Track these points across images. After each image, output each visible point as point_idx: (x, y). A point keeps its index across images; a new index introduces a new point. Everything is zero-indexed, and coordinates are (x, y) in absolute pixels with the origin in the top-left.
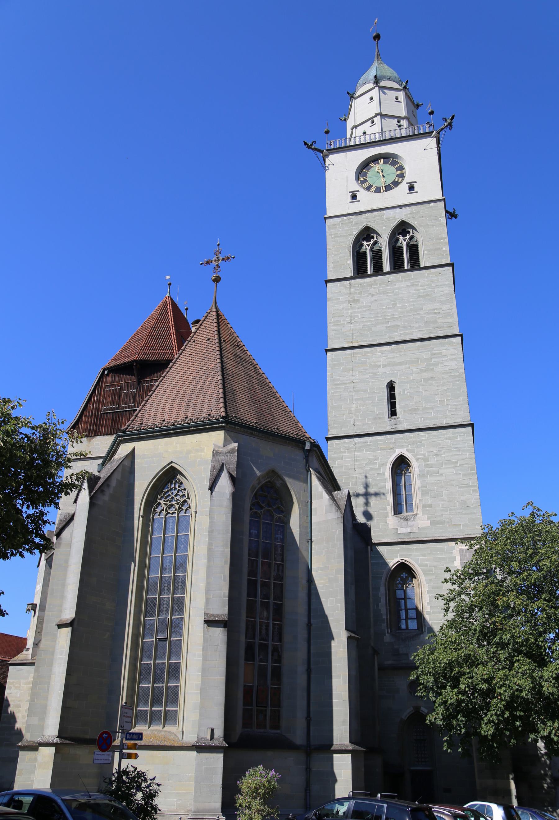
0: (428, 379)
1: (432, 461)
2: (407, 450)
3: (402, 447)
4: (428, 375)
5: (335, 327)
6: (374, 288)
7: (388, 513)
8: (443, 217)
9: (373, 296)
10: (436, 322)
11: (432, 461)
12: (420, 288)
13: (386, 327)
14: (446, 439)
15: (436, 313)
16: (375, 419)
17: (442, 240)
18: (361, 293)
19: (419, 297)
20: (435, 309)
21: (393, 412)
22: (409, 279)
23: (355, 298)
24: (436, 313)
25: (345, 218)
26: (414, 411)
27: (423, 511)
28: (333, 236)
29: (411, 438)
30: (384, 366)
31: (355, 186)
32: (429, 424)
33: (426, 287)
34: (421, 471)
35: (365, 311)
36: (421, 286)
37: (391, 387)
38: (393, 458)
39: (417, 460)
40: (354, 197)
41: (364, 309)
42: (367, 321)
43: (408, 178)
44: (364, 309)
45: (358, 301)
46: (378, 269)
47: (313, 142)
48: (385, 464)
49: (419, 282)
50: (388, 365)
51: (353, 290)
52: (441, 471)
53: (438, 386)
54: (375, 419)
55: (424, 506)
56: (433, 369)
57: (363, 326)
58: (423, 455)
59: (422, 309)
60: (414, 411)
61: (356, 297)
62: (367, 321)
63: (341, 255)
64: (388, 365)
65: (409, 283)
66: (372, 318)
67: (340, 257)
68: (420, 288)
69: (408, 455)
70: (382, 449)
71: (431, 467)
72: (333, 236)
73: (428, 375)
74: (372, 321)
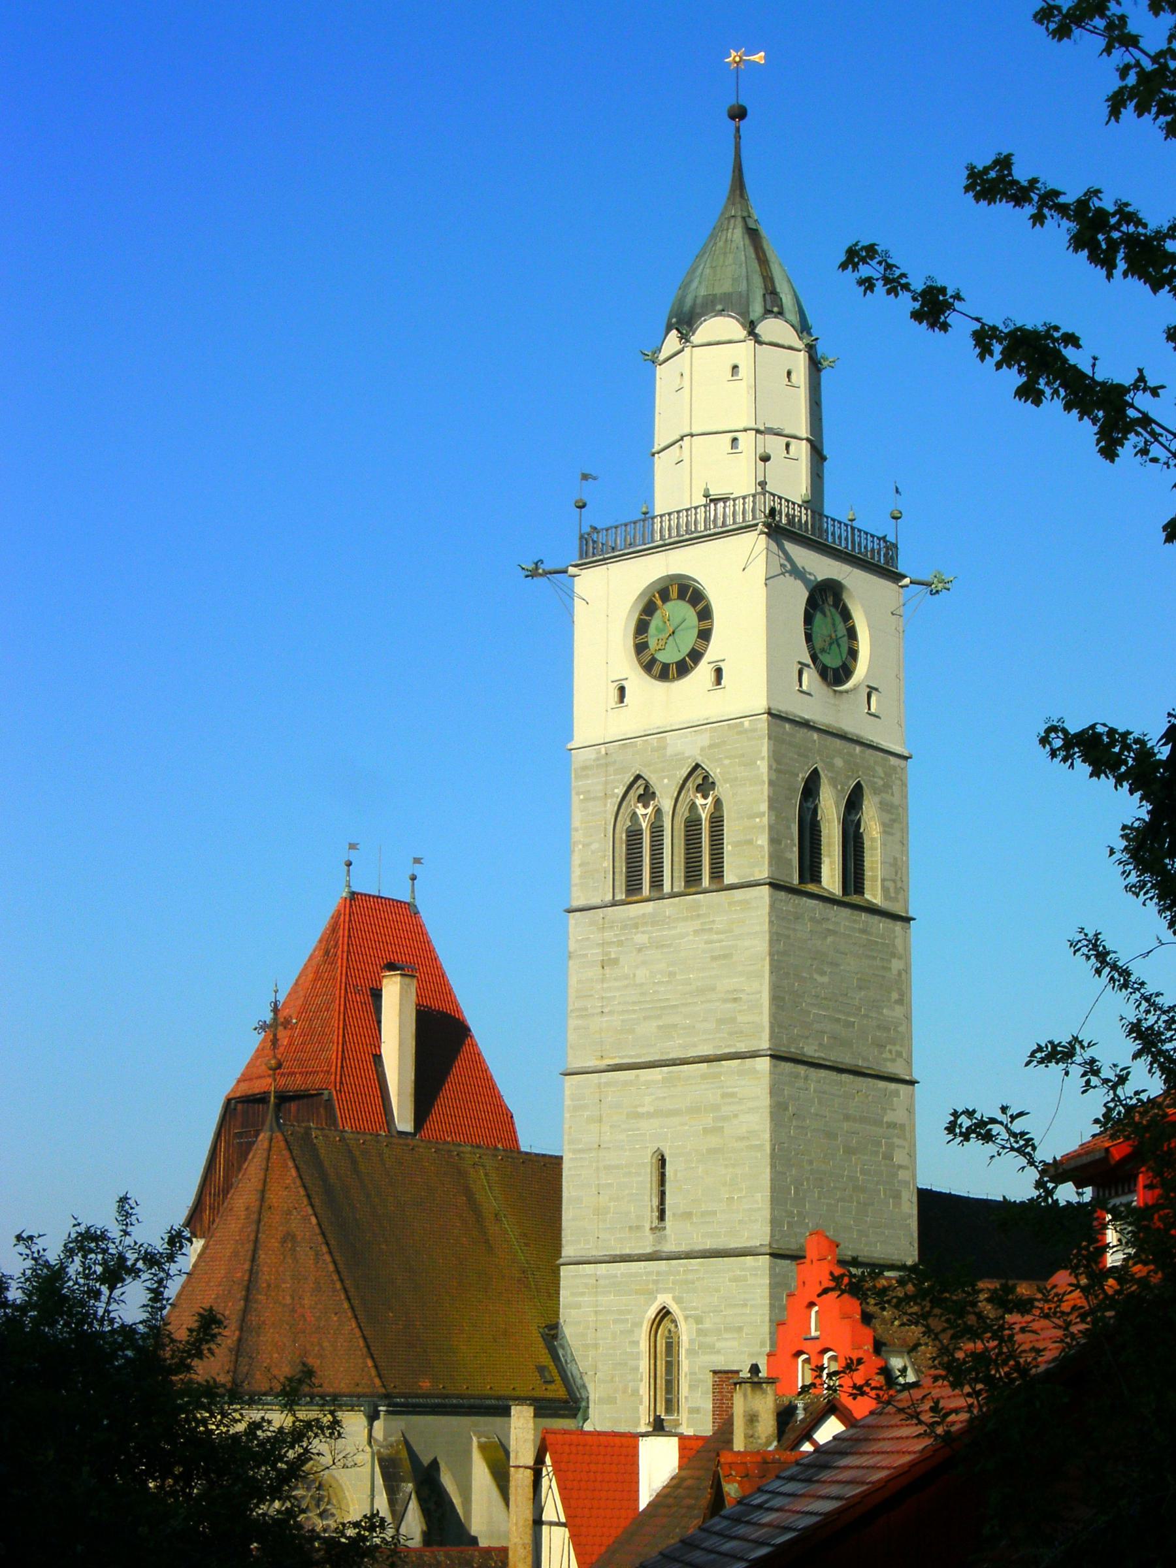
0: (712, 1151)
1: (707, 1325)
2: (674, 1298)
3: (666, 1290)
4: (714, 1141)
5: (579, 1022)
6: (643, 933)
7: (639, 1419)
8: (763, 758)
9: (640, 950)
10: (733, 1020)
11: (707, 1325)
12: (715, 937)
13: (659, 1027)
14: (730, 1280)
15: (735, 1000)
16: (630, 1228)
17: (758, 820)
18: (620, 943)
19: (714, 958)
22: (698, 916)
23: (613, 956)
25: (603, 749)
26: (688, 1215)
27: (688, 1419)
28: (582, 797)
29: (678, 1273)
30: (650, 1115)
32: (709, 1244)
33: (722, 936)
34: (691, 1341)
35: (627, 986)
36: (717, 933)
37: (663, 1161)
39: (686, 1318)
41: (626, 982)
42: (627, 1011)
43: (712, 653)
44: (626, 982)
45: (615, 962)
46: (657, 883)
47: (536, 564)
48: (638, 1325)
49: (713, 921)
50: (657, 1113)
51: (609, 935)
52: (719, 1345)
53: (726, 1166)
54: (630, 1228)
56: (723, 1127)
57: (623, 1021)
58: (695, 1309)
59: (713, 989)
60: (688, 1215)
61: (613, 952)
62: (627, 1011)
63: (595, 846)
64: (657, 1113)
65: (696, 925)
66: (634, 1003)
67: (593, 852)
68: (715, 937)
69: (674, 1308)
70: (637, 1293)
71: (706, 1335)
72: (582, 797)
73: (714, 1141)
74: (635, 1011)
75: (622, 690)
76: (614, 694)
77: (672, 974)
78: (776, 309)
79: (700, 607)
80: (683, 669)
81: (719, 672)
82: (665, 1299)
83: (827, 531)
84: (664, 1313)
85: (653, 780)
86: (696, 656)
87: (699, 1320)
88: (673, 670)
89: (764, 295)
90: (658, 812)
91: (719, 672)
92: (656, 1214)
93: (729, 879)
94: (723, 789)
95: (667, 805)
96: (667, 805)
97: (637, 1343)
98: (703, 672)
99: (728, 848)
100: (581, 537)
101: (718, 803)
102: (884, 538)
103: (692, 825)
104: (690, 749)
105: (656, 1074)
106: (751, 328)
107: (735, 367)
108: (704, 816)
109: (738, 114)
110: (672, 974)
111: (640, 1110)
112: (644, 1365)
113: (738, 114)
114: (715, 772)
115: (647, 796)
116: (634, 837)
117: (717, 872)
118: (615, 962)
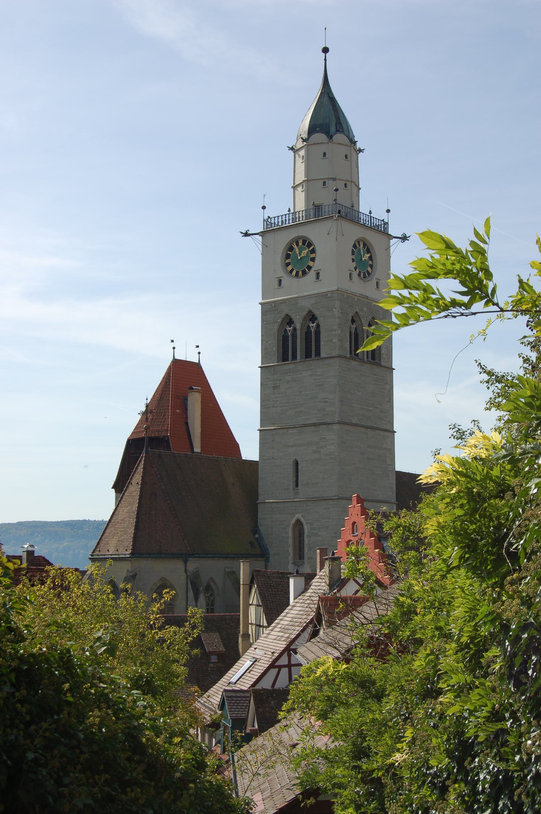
9: (288, 383)
15: (325, 402)
18: (280, 380)
20: (325, 398)
21: (297, 485)
23: (277, 385)
24: (325, 402)
31: (281, 273)
34: (308, 532)
36: (318, 376)
37: (297, 463)
38: (293, 521)
39: (307, 523)
40: (280, 281)
43: (316, 266)
45: (278, 387)
46: (294, 357)
49: (317, 371)
55: (309, 558)
63: (270, 342)
69: (302, 520)
75: (280, 281)
76: (276, 282)
77: (300, 392)
78: (341, 130)
79: (311, 249)
80: (304, 273)
81: (318, 274)
82: (298, 516)
83: (361, 218)
84: (299, 523)
85: (293, 316)
86: (309, 268)
87: (311, 524)
88: (300, 273)
89: (336, 125)
90: (295, 329)
91: (318, 274)
92: (295, 484)
93: (323, 355)
94: (321, 320)
95: (298, 326)
96: (298, 326)
97: (288, 533)
98: (312, 274)
99: (322, 343)
100: (264, 221)
101: (318, 326)
102: (383, 220)
103: (308, 334)
104: (308, 305)
105: (294, 431)
106: (331, 137)
107: (325, 154)
108: (313, 331)
109: (326, 50)
110: (300, 392)
111: (288, 444)
112: (290, 541)
113: (326, 50)
114: (317, 313)
115: (290, 322)
116: (285, 339)
117: (318, 353)
118: (279, 387)
